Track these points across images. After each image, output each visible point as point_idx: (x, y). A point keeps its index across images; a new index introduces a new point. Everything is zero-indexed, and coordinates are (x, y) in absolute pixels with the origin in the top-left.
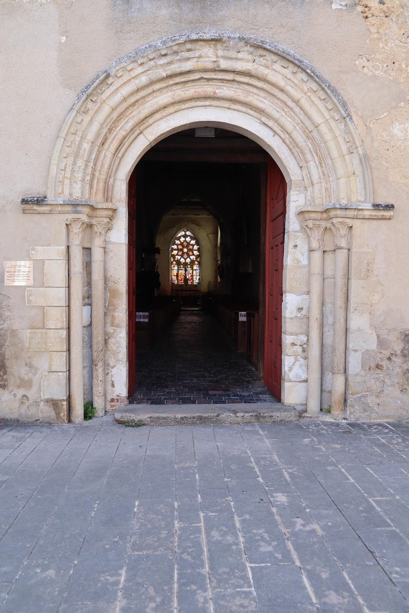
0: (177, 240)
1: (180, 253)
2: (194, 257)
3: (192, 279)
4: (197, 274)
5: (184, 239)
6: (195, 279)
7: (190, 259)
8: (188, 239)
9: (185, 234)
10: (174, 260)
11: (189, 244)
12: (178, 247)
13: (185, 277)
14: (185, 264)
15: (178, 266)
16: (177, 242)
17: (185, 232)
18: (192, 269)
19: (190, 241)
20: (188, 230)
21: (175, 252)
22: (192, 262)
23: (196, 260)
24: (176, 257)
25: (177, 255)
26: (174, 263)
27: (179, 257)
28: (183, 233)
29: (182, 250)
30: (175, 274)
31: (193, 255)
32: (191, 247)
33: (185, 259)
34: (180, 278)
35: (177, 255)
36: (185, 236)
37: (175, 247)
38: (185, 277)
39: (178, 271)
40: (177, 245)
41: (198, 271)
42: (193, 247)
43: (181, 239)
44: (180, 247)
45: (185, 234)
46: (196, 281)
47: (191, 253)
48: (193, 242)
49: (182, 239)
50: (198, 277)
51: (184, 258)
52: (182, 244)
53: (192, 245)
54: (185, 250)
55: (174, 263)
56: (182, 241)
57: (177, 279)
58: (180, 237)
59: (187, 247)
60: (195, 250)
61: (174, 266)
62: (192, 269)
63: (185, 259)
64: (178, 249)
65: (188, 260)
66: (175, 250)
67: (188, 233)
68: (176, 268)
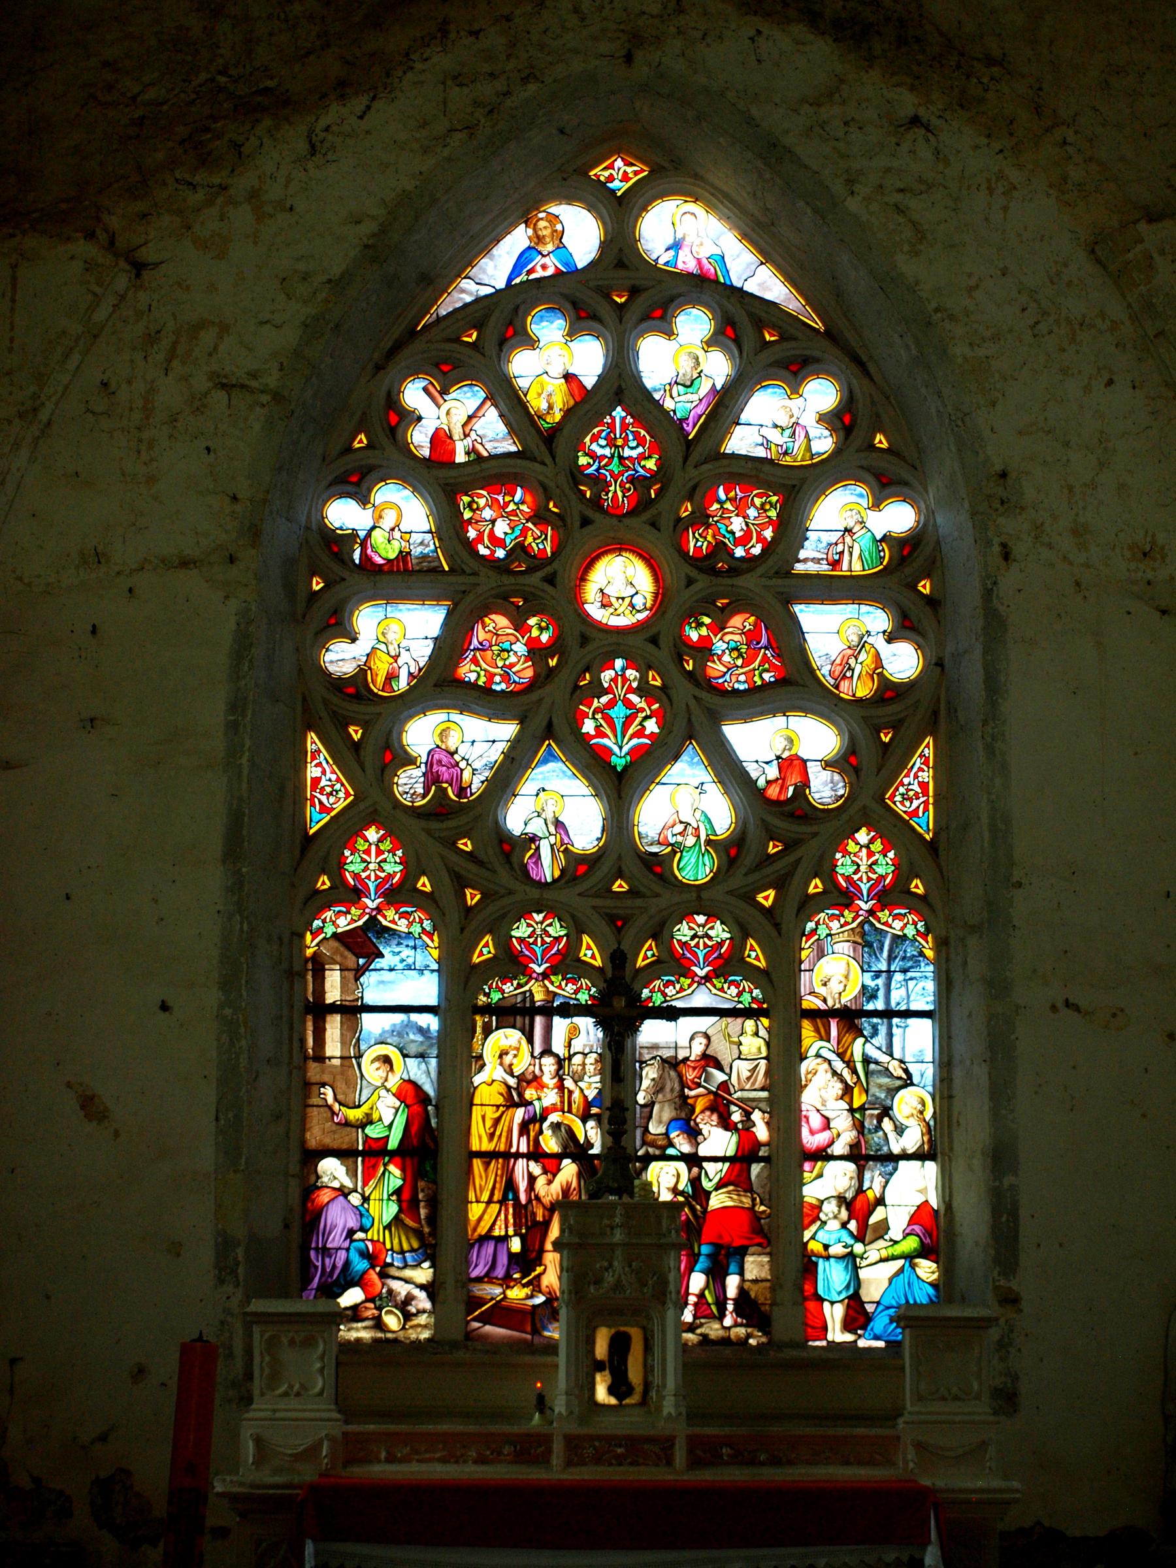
0: (447, 376)
1: (505, 649)
2: (817, 739)
3: (777, 1221)
4: (871, 1113)
5: (589, 358)
6: (829, 1234)
7: (728, 769)
8: (679, 359)
9: (620, 248)
10: (373, 805)
11: (694, 454)
12: (450, 526)
13: (614, 1171)
14: (624, 892)
15: (456, 931)
16: (447, 414)
17: (620, 214)
18: (783, 1011)
19: (725, 406)
20: (670, 175)
21: (394, 636)
22: (780, 841)
23: (866, 805)
24: (419, 734)
25: (440, 684)
26: (373, 859)
27: (481, 740)
28: (581, 234)
29: (540, 585)
30: (389, 1119)
31: (795, 685)
32: (742, 523)
33: (620, 787)
34: (482, 1213)
35: (440, 684)
36: (622, 295)
37: (394, 520)
38: (614, 1171)
39: (456, 1055)
40: (446, 479)
41: (917, 1041)
42: (790, 528)
43: (523, 366)
44: (500, 523)
45: (620, 248)
46: (874, 1246)
47: (729, 651)
48: (788, 417)
49: (555, 360)
50: (912, 1187)
51: (593, 764)
52: (544, 451)
53: (754, 473)
54: (619, 586)
55: (373, 859)
56: (546, 396)
57: (431, 1218)
58: (504, 320)
59: (648, 521)
60: (834, 588)
61: (363, 946)
62: (783, 1011)
63: (620, 787)
64: (461, 580)
65: (685, 806)
66: (400, 579)
67: (683, 231)
68: (405, 979)
